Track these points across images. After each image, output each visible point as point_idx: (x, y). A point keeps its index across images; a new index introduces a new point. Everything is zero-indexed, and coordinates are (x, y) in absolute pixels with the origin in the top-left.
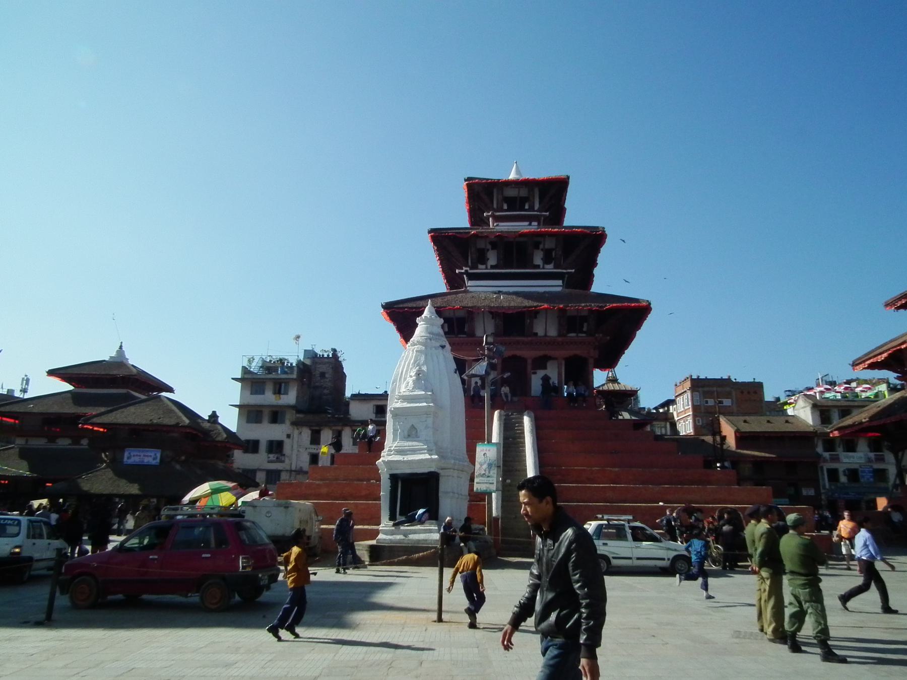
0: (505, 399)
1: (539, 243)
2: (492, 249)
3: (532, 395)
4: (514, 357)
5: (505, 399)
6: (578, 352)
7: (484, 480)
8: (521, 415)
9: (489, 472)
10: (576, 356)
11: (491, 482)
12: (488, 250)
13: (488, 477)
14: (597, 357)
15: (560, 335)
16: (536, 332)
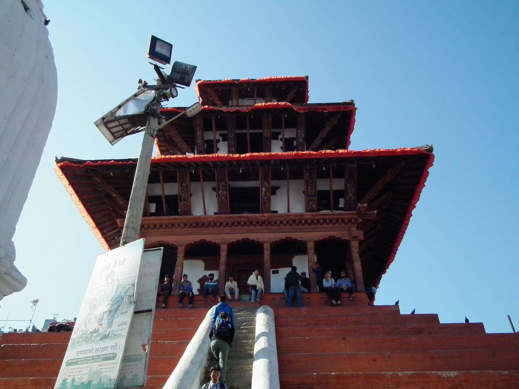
0: (229, 296)
1: (279, 133)
2: (223, 141)
3: (271, 292)
4: (245, 242)
5: (229, 296)
6: (336, 234)
7: (90, 351)
8: (254, 312)
9: (110, 324)
10: (332, 240)
11: (109, 351)
12: (218, 141)
13: (106, 337)
14: (362, 238)
15: (307, 210)
16: (275, 210)
